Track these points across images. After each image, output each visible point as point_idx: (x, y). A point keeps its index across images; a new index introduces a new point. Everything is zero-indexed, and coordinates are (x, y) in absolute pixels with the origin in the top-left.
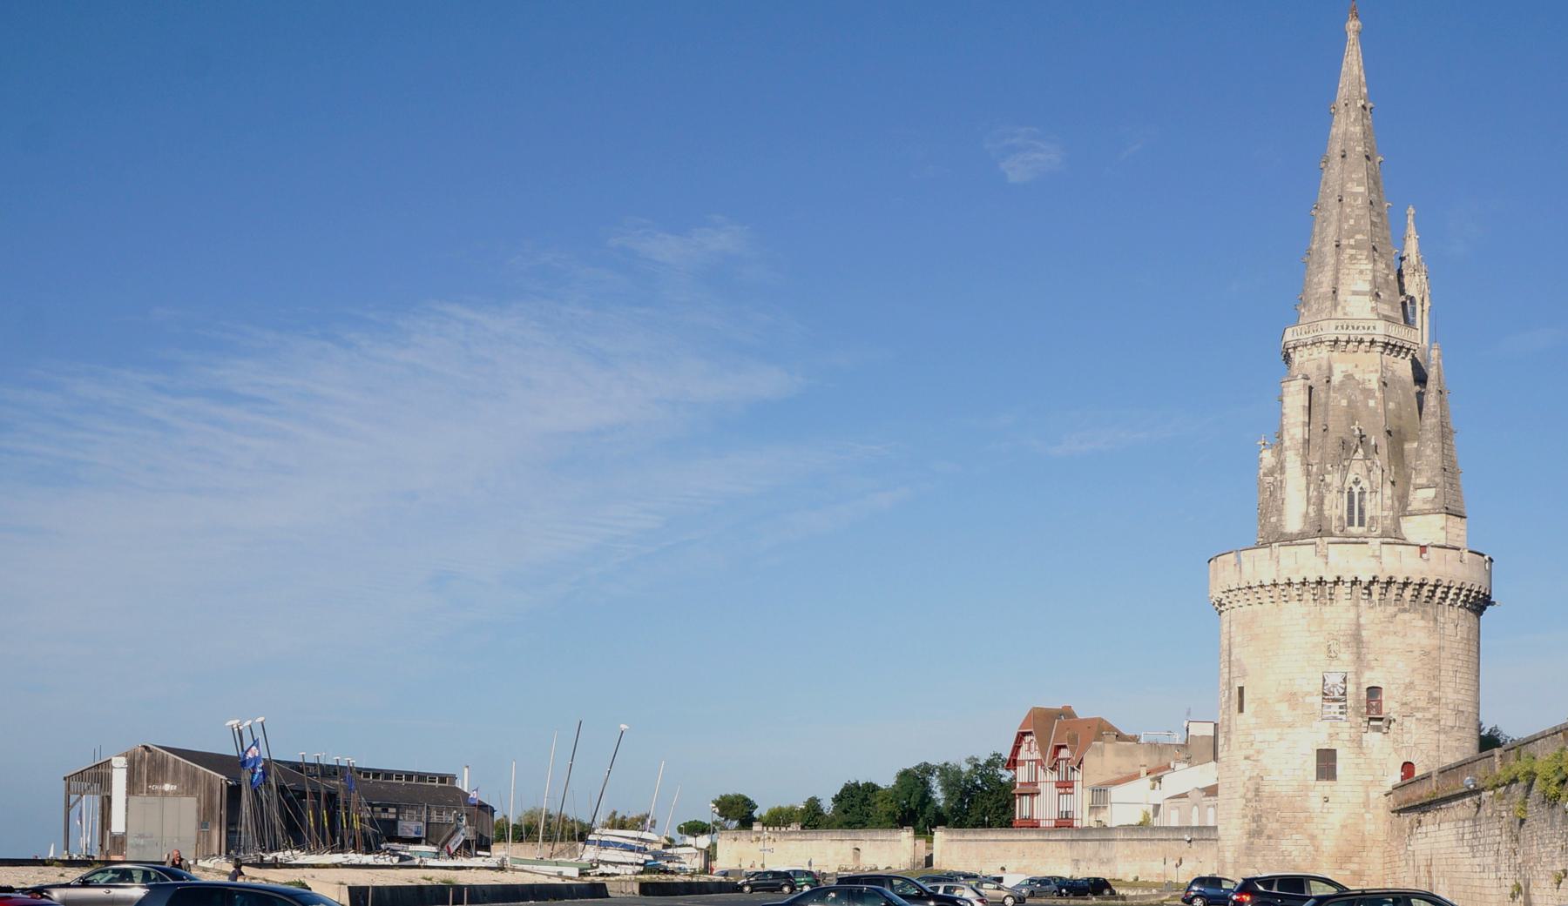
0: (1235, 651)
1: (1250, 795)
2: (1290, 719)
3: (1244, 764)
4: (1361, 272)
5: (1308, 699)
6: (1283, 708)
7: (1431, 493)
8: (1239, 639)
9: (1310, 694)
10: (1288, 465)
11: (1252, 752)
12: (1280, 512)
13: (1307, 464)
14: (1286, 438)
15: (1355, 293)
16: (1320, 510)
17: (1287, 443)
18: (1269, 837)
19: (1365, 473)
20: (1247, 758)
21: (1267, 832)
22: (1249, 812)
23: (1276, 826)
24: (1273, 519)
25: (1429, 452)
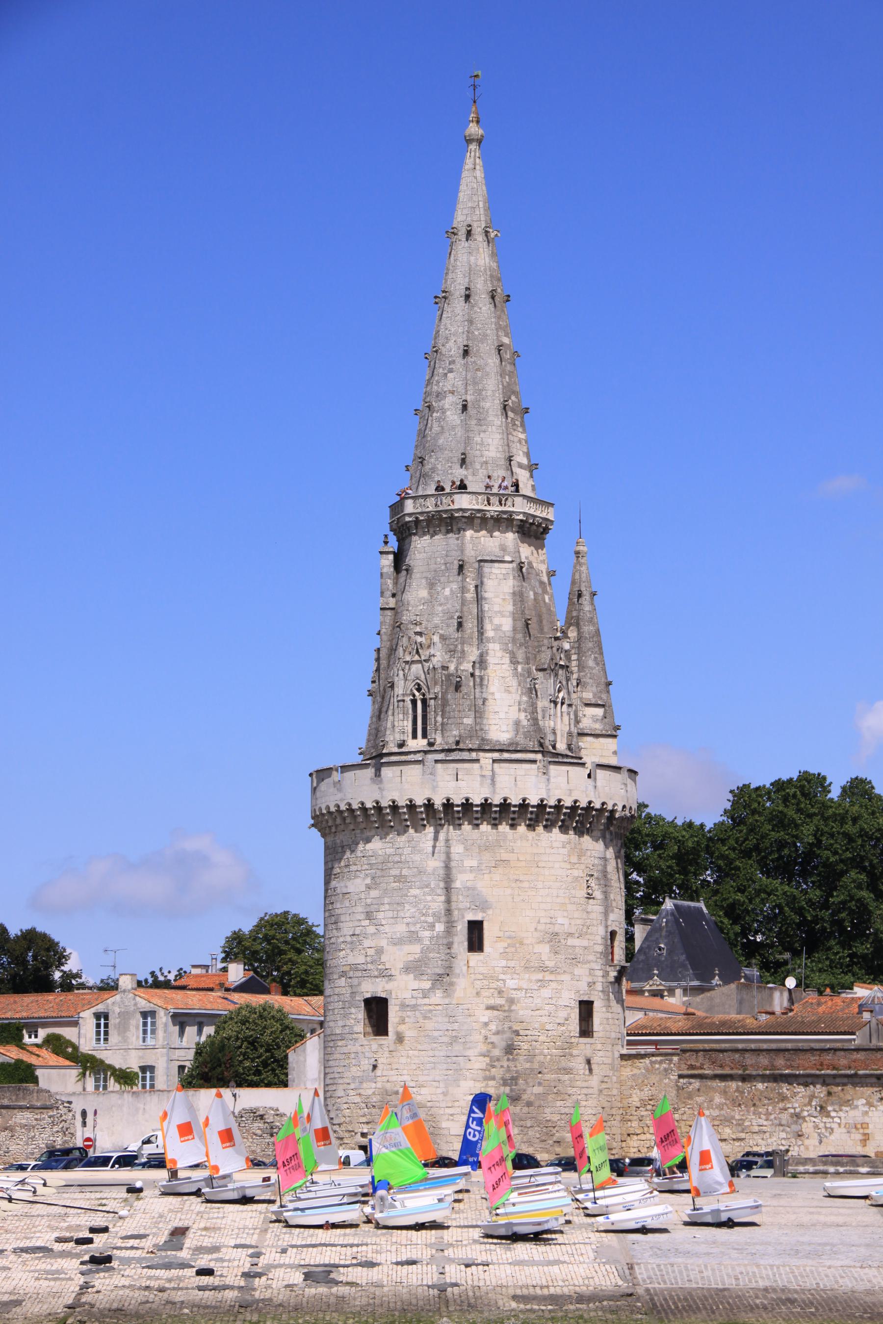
0: (460, 881)
1: (497, 1052)
2: (550, 964)
3: (485, 1016)
4: (520, 441)
5: (571, 941)
6: (544, 950)
7: (600, 712)
8: (470, 863)
9: (571, 935)
10: (491, 660)
11: (500, 1001)
12: (479, 713)
13: (514, 662)
14: (488, 626)
15: (520, 466)
16: (535, 721)
17: (489, 633)
18: (529, 1104)
19: (564, 683)
20: (490, 1008)
21: (525, 1097)
22: (497, 1072)
23: (537, 1090)
24: (468, 721)
25: (591, 663)
